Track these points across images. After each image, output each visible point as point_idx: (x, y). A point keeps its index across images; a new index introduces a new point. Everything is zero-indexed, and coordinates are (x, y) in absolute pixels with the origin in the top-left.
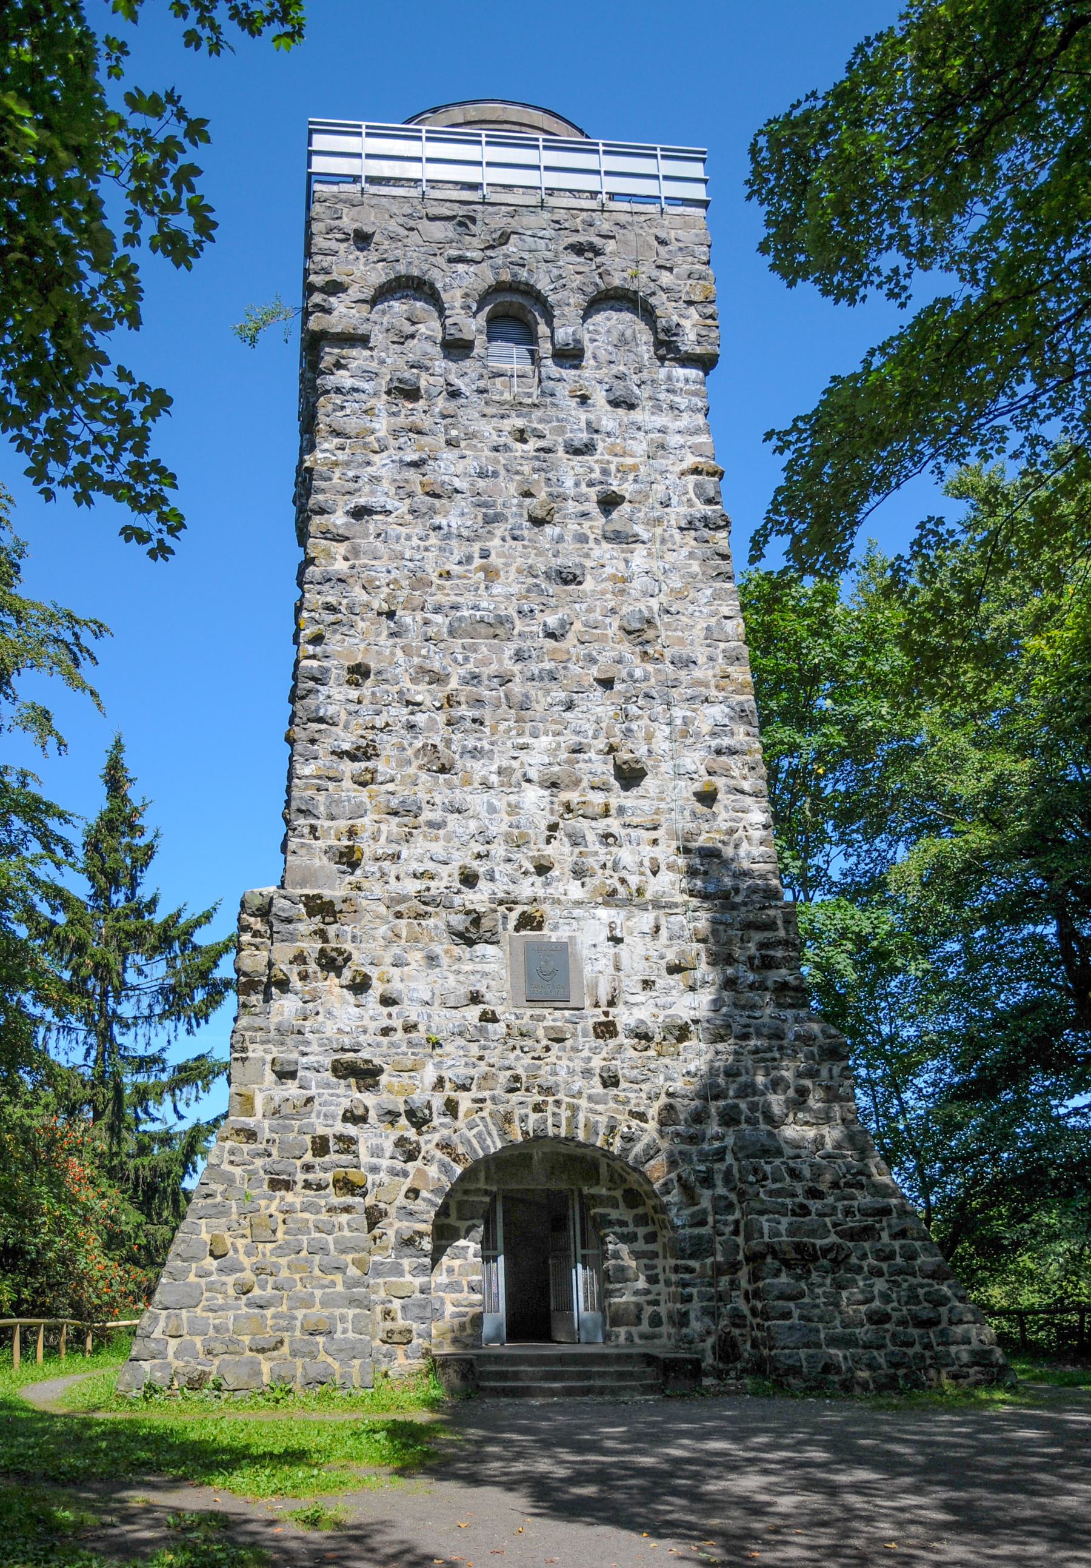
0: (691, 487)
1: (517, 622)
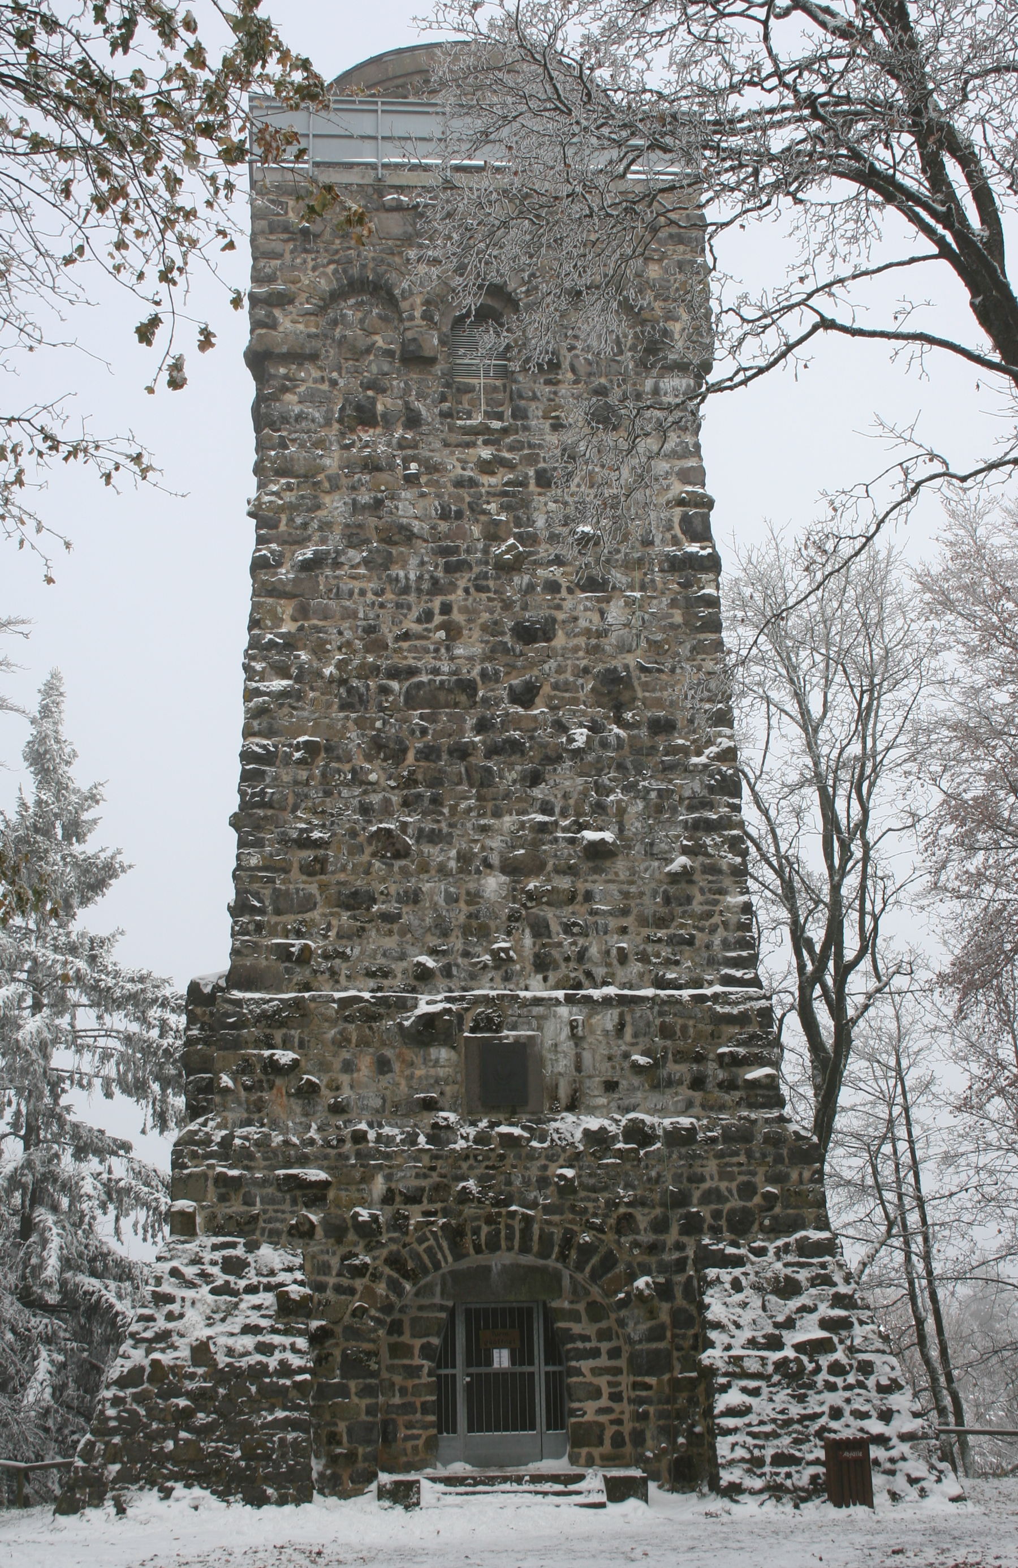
0: (676, 520)
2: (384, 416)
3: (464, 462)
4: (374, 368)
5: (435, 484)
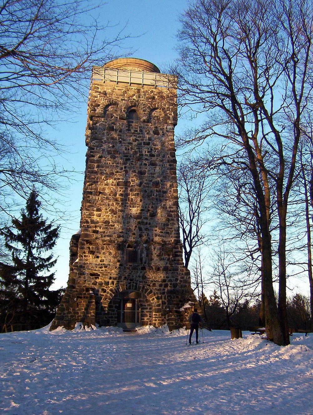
1: (131, 183)
5: (124, 143)
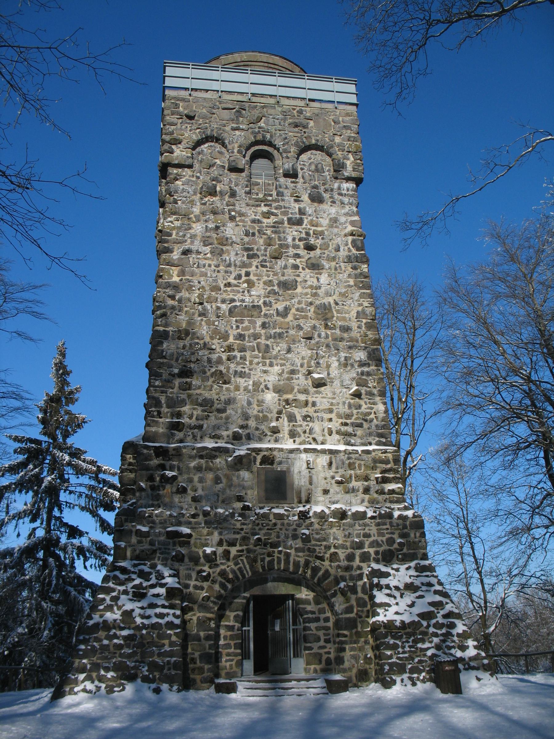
0: (350, 242)
1: (264, 309)
2: (220, 192)
3: (256, 213)
4: (216, 173)
5: (243, 221)
